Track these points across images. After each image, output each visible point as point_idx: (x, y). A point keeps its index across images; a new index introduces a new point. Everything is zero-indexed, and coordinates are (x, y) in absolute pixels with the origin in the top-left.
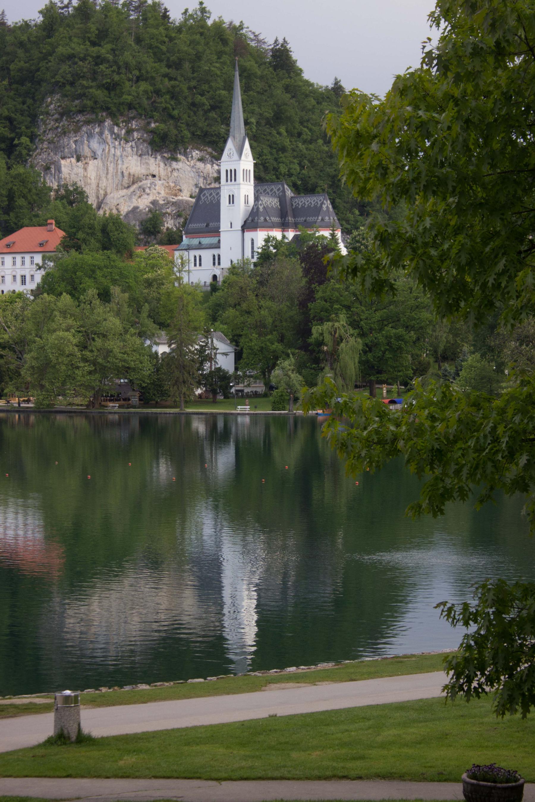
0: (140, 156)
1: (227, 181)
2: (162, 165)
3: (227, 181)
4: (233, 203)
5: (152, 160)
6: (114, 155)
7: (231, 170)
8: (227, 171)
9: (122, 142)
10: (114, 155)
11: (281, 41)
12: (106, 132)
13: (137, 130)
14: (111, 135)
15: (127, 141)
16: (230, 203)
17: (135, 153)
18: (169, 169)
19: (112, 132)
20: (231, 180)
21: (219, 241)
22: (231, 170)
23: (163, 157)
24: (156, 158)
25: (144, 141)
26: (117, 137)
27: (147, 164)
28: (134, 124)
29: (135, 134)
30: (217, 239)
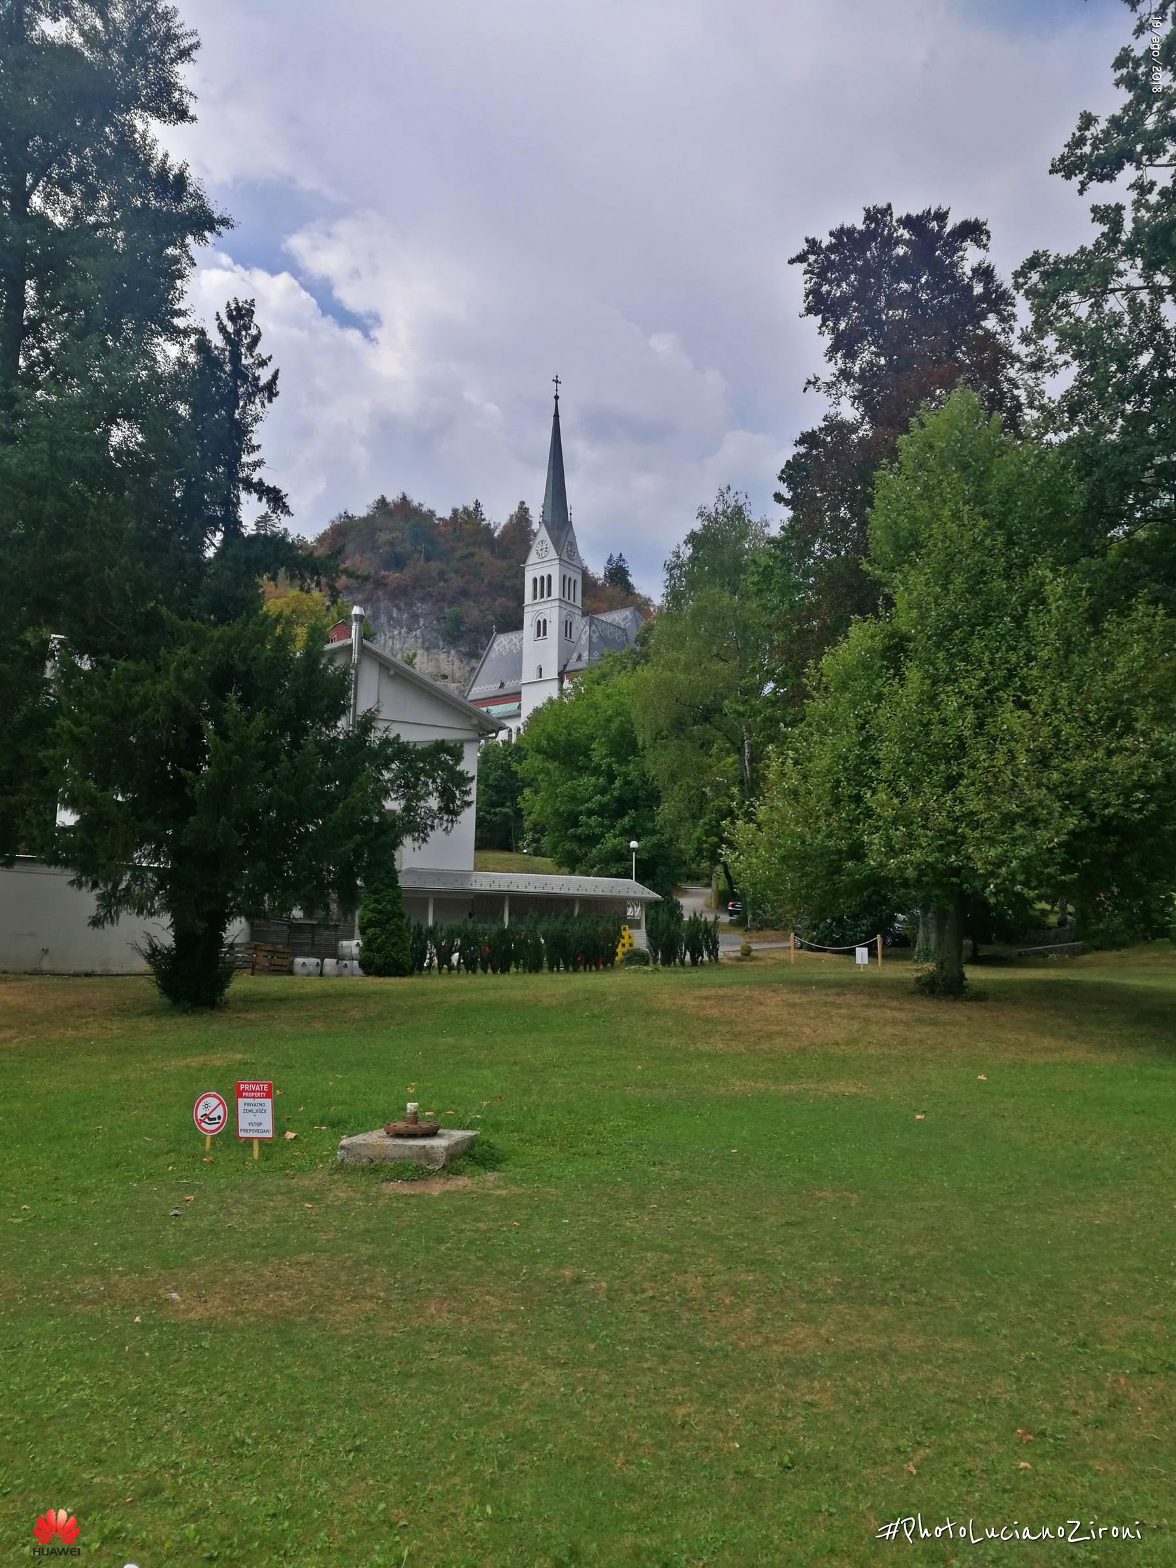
0: (427, 649)
1: (535, 598)
2: (457, 663)
3: (535, 598)
4: (545, 634)
5: (443, 656)
6: (392, 648)
7: (542, 578)
8: (535, 580)
9: (403, 631)
10: (392, 648)
11: (615, 558)
12: (383, 619)
13: (426, 616)
14: (389, 621)
15: (410, 630)
16: (539, 635)
17: (419, 644)
18: (468, 668)
19: (390, 618)
20: (542, 596)
21: (519, 707)
22: (542, 578)
23: (458, 652)
24: (449, 652)
25: (433, 630)
26: (398, 623)
27: (437, 660)
28: (420, 608)
29: (422, 622)
30: (516, 704)
